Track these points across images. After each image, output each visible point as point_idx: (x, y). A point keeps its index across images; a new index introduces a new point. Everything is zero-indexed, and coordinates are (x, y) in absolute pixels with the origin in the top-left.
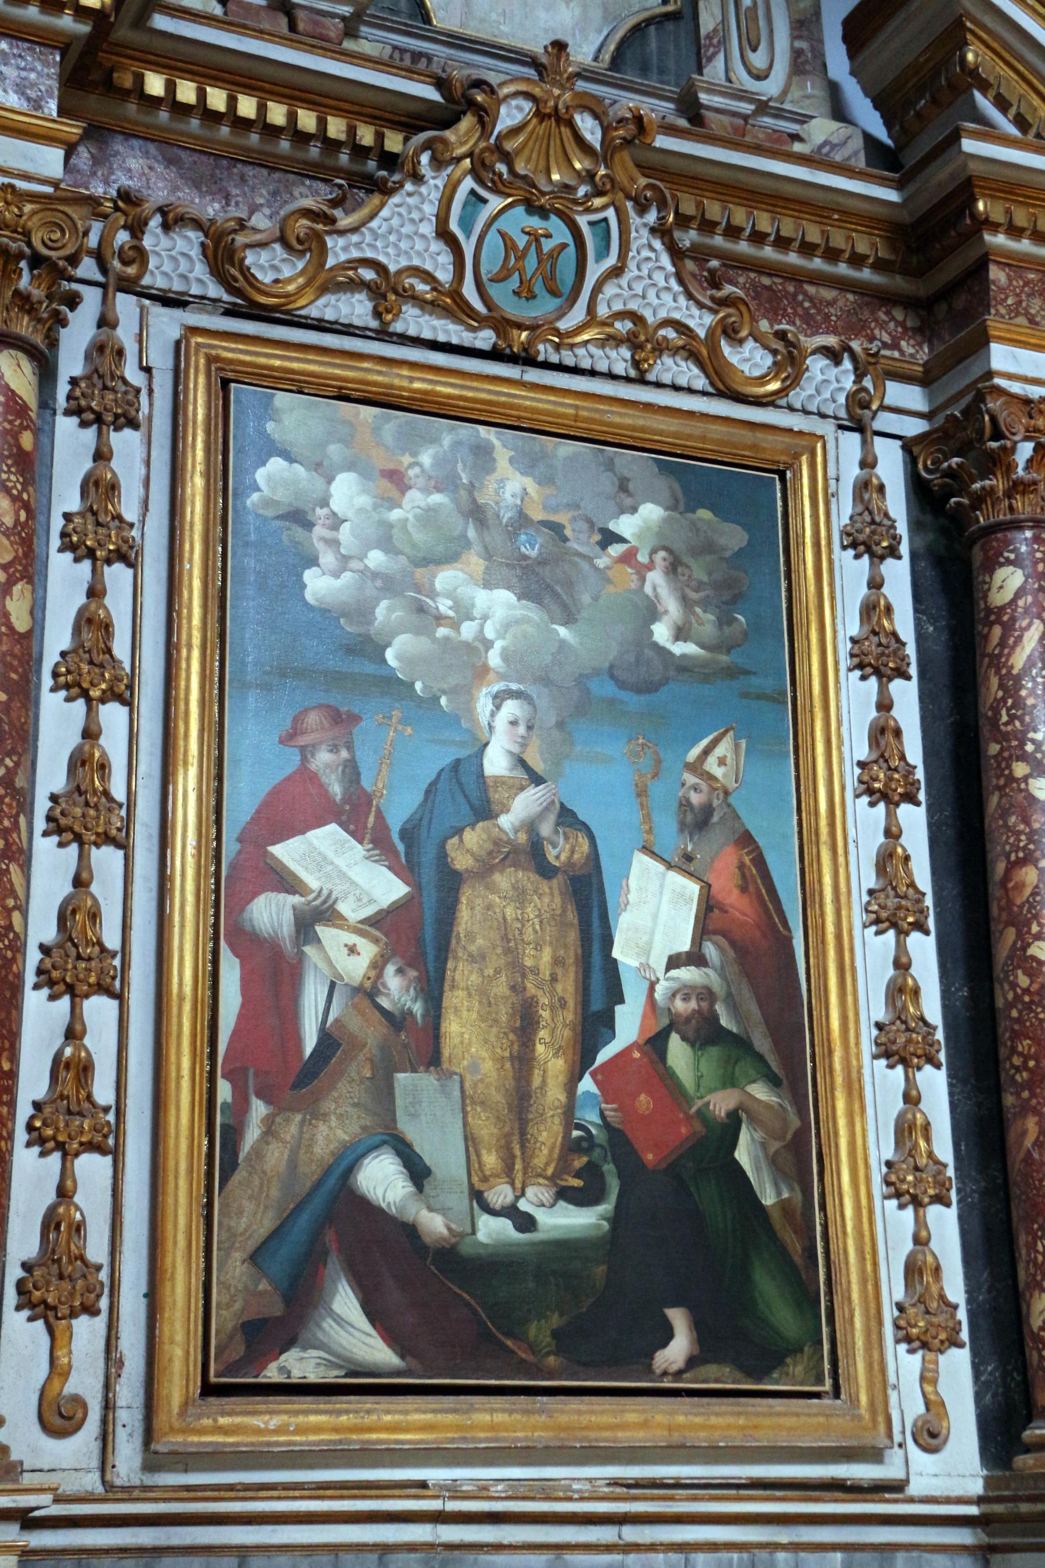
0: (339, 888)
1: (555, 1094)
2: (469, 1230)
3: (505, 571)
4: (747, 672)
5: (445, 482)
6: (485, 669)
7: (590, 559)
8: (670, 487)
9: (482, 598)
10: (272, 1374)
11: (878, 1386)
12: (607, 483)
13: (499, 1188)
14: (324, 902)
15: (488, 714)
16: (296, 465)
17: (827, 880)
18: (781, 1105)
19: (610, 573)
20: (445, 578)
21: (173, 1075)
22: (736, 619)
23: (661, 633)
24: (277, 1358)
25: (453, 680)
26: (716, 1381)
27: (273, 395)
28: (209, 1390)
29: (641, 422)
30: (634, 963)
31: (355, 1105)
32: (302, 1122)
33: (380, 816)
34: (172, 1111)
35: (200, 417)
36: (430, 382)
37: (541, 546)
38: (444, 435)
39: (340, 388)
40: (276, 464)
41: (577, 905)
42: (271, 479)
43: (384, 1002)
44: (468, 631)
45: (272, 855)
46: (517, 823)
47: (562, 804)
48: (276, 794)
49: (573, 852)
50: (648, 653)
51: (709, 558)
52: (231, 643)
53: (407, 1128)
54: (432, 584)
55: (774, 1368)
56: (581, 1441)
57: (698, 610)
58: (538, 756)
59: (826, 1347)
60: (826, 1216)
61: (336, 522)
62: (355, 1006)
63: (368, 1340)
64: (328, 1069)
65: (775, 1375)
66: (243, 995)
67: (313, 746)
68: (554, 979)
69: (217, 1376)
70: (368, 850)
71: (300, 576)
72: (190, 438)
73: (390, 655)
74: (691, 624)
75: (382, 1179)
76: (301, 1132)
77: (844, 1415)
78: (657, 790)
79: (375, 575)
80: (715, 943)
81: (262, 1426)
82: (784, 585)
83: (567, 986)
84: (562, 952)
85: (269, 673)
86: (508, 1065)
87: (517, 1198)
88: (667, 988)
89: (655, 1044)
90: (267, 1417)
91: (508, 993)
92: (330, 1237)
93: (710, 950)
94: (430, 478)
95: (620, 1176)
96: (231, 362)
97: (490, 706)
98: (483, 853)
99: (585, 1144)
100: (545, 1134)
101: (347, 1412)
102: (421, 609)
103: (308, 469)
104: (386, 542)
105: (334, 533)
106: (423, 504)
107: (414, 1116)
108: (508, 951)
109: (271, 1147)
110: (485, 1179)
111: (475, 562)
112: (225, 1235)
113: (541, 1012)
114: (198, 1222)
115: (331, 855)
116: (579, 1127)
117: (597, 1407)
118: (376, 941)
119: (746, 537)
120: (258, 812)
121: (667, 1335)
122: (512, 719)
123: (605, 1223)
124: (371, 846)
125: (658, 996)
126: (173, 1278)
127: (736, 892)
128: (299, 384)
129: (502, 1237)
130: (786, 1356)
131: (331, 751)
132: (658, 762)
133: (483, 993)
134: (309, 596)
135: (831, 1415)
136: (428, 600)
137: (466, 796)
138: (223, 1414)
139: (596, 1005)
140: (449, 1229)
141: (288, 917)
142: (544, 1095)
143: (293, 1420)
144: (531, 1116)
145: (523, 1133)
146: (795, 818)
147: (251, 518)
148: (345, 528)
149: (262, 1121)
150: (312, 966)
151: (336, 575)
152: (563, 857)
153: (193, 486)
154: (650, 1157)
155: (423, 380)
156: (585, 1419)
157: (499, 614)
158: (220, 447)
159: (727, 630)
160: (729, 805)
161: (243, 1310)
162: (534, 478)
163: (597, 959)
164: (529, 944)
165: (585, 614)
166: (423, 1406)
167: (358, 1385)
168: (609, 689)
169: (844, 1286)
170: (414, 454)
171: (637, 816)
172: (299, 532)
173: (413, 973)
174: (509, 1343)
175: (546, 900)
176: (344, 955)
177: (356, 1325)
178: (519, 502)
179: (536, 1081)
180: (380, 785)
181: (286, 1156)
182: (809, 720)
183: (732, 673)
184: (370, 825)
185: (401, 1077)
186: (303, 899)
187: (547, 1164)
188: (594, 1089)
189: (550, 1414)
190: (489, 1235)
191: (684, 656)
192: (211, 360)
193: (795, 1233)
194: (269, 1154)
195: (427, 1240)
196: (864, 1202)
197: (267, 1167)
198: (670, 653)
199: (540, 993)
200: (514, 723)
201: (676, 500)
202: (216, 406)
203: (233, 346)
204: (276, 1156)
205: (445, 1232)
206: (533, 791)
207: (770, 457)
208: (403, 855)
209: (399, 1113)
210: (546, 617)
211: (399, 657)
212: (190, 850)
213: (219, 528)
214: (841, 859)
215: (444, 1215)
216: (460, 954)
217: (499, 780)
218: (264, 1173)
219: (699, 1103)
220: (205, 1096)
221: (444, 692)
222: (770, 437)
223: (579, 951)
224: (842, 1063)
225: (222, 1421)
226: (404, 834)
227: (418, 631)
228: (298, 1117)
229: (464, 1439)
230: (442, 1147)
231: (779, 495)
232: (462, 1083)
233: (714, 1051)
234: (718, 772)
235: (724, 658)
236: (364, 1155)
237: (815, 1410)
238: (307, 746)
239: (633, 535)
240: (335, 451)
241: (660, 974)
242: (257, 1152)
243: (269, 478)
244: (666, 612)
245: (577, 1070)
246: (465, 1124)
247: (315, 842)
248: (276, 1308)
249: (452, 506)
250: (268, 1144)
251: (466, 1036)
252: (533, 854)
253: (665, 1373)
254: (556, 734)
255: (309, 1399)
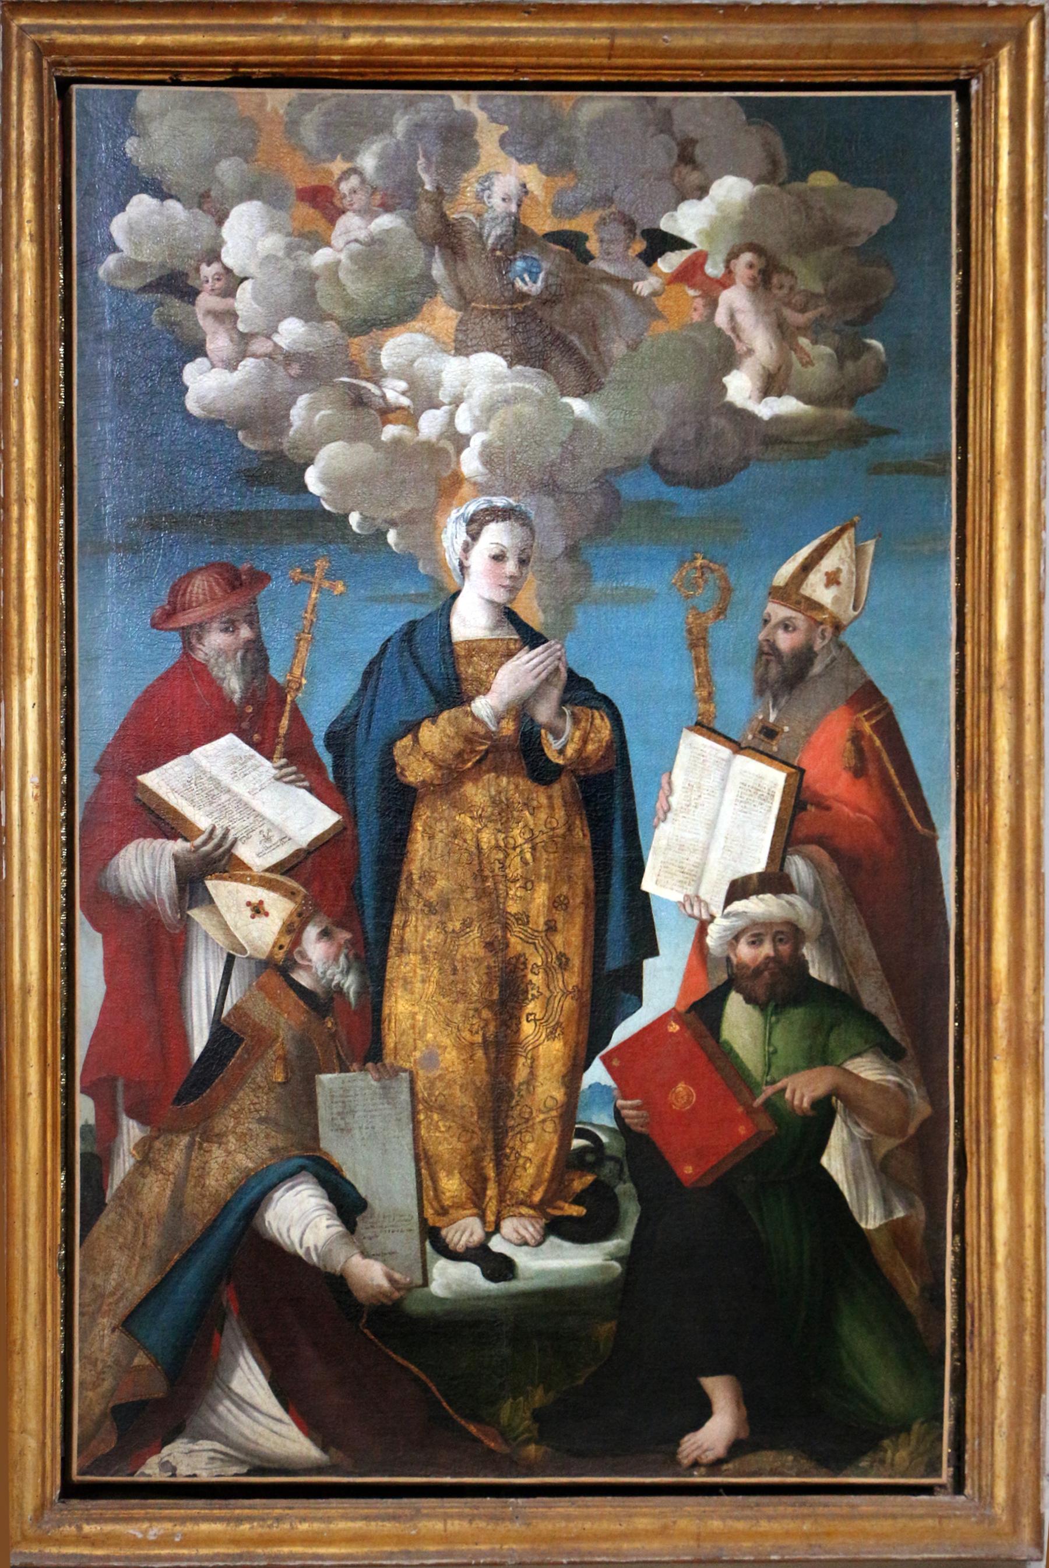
0: (239, 825)
1: (549, 1090)
2: (419, 1281)
3: (489, 323)
4: (886, 432)
5: (399, 193)
6: (457, 480)
7: (625, 284)
8: (766, 144)
9: (453, 370)
10: (152, 1471)
11: (1027, 1476)
12: (660, 152)
13: (462, 1223)
14: (219, 846)
15: (459, 548)
16: (171, 203)
17: (1003, 744)
18: (899, 1085)
19: (659, 302)
20: (397, 347)
21: (18, 1092)
22: (869, 348)
23: (740, 387)
24: (159, 1452)
25: (408, 503)
26: (773, 1473)
27: (135, 94)
28: (71, 1491)
29: (719, 40)
30: (676, 896)
31: (261, 1121)
32: (190, 1147)
33: (297, 716)
34: (18, 1139)
35: (28, 147)
36: (378, 31)
37: (549, 273)
38: (397, 115)
39: (236, 65)
40: (142, 204)
41: (590, 819)
42: (138, 228)
43: (303, 979)
44: (430, 424)
45: (144, 786)
46: (501, 708)
47: (571, 673)
48: (148, 699)
49: (585, 741)
50: (719, 422)
51: (826, 252)
52: (81, 488)
53: (335, 1147)
54: (376, 358)
55: (864, 1453)
56: (569, 1554)
57: (804, 341)
58: (535, 603)
59: (947, 1423)
60: (963, 1241)
61: (231, 281)
62: (261, 987)
63: (277, 1427)
64: (226, 1074)
65: (864, 1464)
66: (108, 982)
67: (201, 626)
68: (551, 928)
69: (81, 1473)
70: (281, 767)
71: (178, 374)
72: (14, 184)
73: (312, 479)
74: (789, 366)
75: (299, 1217)
76: (188, 1158)
77: (968, 1517)
78: (724, 635)
79: (289, 358)
80: (806, 857)
81: (140, 1536)
82: (955, 278)
83: (571, 938)
84: (565, 889)
85: (136, 526)
86: (480, 1054)
87: (489, 1235)
88: (726, 929)
89: (704, 1011)
90: (145, 1525)
91: (482, 952)
92: (228, 1296)
93: (798, 868)
94: (375, 190)
95: (641, 1199)
96: (72, 49)
97: (463, 537)
98: (449, 756)
99: (590, 1158)
100: (531, 1146)
101: (250, 1519)
102: (359, 401)
103: (187, 206)
104: (306, 306)
105: (229, 300)
106: (362, 235)
107: (345, 1130)
108: (482, 894)
109: (148, 1180)
110: (443, 1211)
111: (443, 315)
112: (88, 1297)
113: (530, 976)
114: (54, 1280)
115: (226, 779)
116: (582, 1134)
117: (593, 1511)
118: (291, 894)
119: (893, 206)
120: (123, 727)
121: (703, 1411)
122: (496, 551)
123: (616, 1265)
124: (283, 761)
125: (710, 941)
126: (23, 1351)
127: (846, 777)
128: (174, 71)
129: (465, 1288)
130: (882, 1437)
131: (226, 630)
132: (727, 591)
133: (444, 954)
134: (192, 404)
135: (948, 1517)
136: (370, 386)
137: (424, 676)
138: (89, 1520)
139: (615, 960)
140: (391, 1280)
141: (167, 871)
142: (531, 1093)
143: (178, 1528)
144: (512, 1123)
145: (499, 1147)
146: (953, 654)
147: (104, 295)
148: (245, 291)
149: (136, 1146)
150: (201, 937)
151: (231, 366)
152: (570, 751)
153: (20, 258)
154: (689, 1170)
155: (365, 30)
156: (575, 1527)
157: (480, 391)
158: (58, 191)
159: (850, 366)
160: (841, 646)
161: (113, 1390)
162: (540, 164)
163: (617, 895)
164: (515, 881)
165: (615, 373)
166: (351, 1512)
167: (265, 1484)
168: (652, 487)
169: (985, 1339)
170: (351, 156)
171: (689, 677)
172: (176, 306)
173: (344, 936)
174: (472, 1429)
175: (543, 815)
176: (248, 916)
177: (264, 1408)
178: (513, 208)
179: (521, 1073)
180: (297, 672)
181: (168, 1192)
182: (986, 496)
183: (855, 436)
184: (282, 731)
185: (326, 1079)
186: (188, 845)
187: (533, 1187)
188: (607, 1080)
189: (527, 1520)
190: (448, 1286)
191: (777, 420)
192: (41, 50)
193: (911, 1266)
194: (146, 1190)
195: (361, 1296)
196: (1029, 1218)
197: (144, 1208)
198: (752, 417)
199: (529, 950)
200: (499, 558)
201: (774, 163)
202: (51, 124)
203: (74, 22)
204: (155, 1192)
205: (385, 1284)
206: (527, 657)
207: (941, 61)
208: (330, 770)
209: (324, 1129)
210: (552, 386)
211: (324, 480)
212: (32, 790)
213: (60, 319)
214: (1029, 711)
215: (384, 1261)
216: (412, 904)
217: (474, 647)
218: (140, 1214)
219: (769, 1091)
220: (60, 1119)
221: (393, 523)
222: (944, 26)
223: (591, 886)
224: (1008, 1019)
225: (87, 1529)
226: (332, 740)
227: (353, 436)
228: (185, 1140)
229: (407, 1554)
230: (384, 1173)
231: (955, 124)
232: (412, 1082)
233: (797, 1015)
234: (825, 596)
235: (844, 414)
236: (273, 1187)
237: (920, 1511)
238: (191, 627)
239: (699, 233)
240: (228, 170)
241: (717, 909)
242: (131, 1189)
243: (131, 229)
244: (750, 352)
245: (583, 1054)
246: (416, 1138)
247: (204, 763)
248: (157, 1388)
249: (409, 230)
250: (144, 1176)
251: (420, 1017)
252: (523, 750)
253: (696, 1464)
254: (565, 568)
255: (200, 1502)
